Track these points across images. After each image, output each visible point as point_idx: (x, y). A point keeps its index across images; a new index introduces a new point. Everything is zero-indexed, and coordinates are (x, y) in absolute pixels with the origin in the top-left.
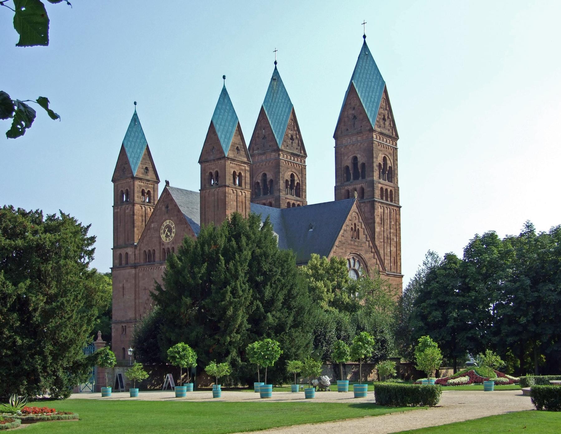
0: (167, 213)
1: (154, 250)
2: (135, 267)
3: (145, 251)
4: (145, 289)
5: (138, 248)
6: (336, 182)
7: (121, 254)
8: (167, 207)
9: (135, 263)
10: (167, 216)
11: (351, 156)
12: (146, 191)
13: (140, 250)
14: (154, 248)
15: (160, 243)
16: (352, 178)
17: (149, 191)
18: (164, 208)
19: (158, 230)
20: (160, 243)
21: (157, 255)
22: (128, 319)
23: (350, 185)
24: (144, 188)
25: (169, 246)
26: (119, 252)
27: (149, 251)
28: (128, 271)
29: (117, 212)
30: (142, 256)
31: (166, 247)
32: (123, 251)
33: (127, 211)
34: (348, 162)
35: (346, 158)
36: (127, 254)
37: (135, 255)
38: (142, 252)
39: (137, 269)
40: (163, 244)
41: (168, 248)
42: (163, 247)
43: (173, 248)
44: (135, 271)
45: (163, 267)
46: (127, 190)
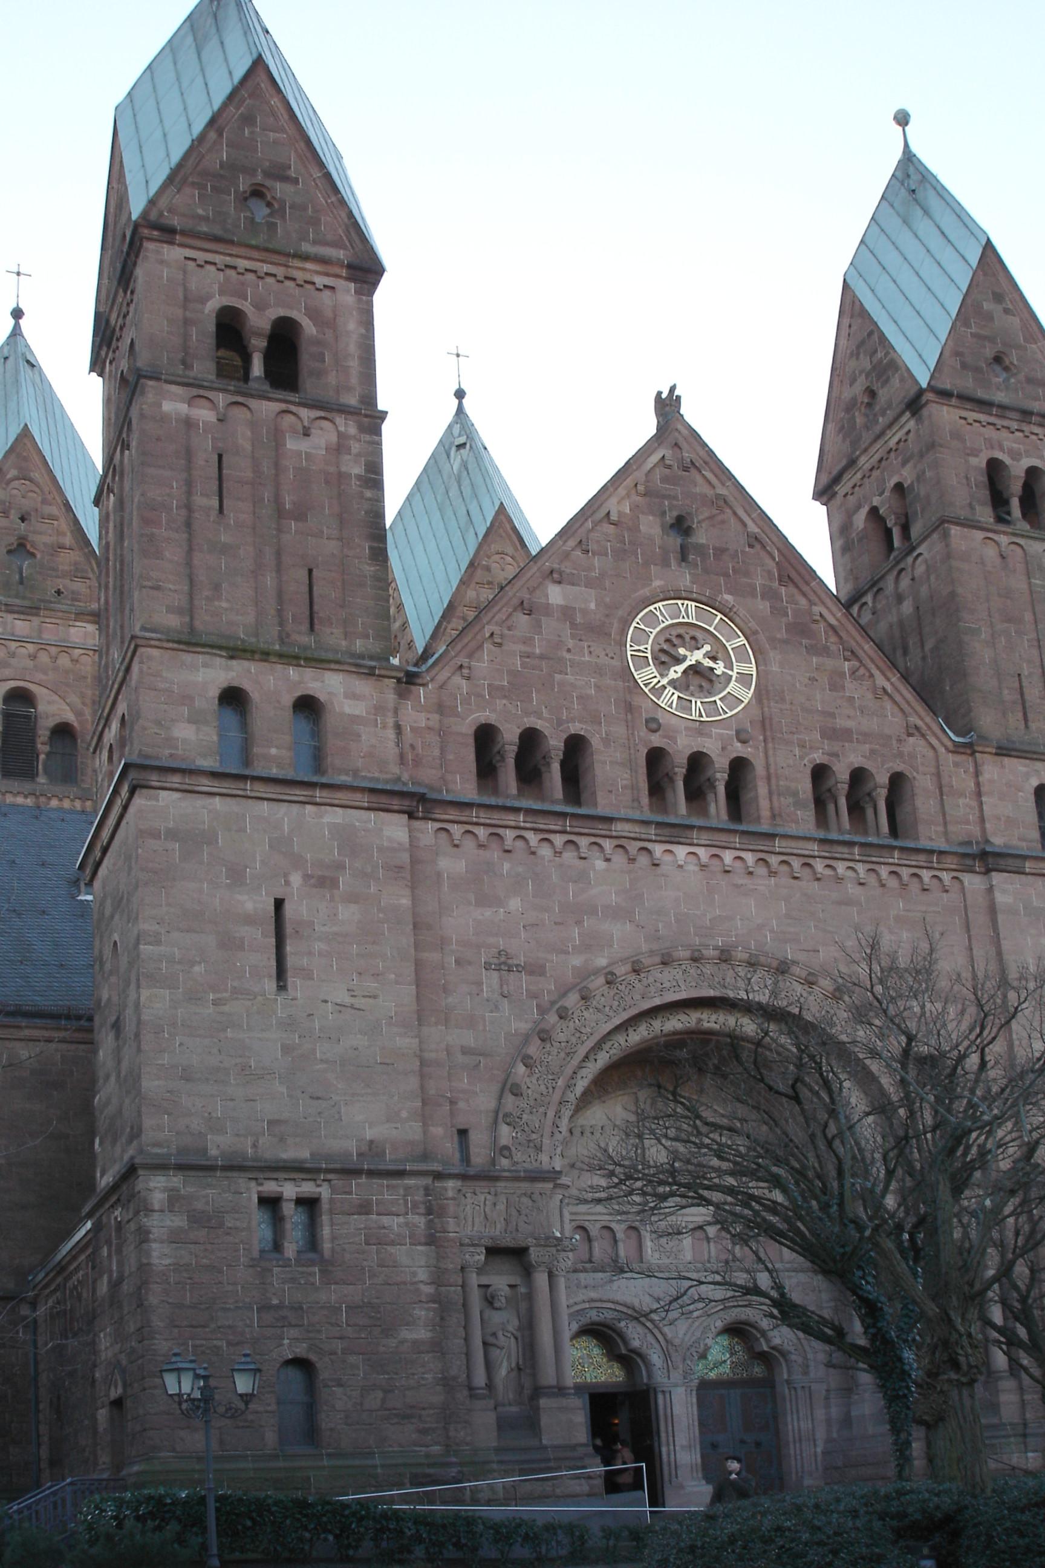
4: (504, 964)
8: (681, 526)
14: (576, 728)
15: (629, 708)
18: (650, 527)
19: (607, 630)
22: (352, 1146)
25: (710, 746)
27: (530, 739)
28: (335, 816)
40: (653, 725)
42: (656, 740)
43: (739, 767)
45: (681, 851)
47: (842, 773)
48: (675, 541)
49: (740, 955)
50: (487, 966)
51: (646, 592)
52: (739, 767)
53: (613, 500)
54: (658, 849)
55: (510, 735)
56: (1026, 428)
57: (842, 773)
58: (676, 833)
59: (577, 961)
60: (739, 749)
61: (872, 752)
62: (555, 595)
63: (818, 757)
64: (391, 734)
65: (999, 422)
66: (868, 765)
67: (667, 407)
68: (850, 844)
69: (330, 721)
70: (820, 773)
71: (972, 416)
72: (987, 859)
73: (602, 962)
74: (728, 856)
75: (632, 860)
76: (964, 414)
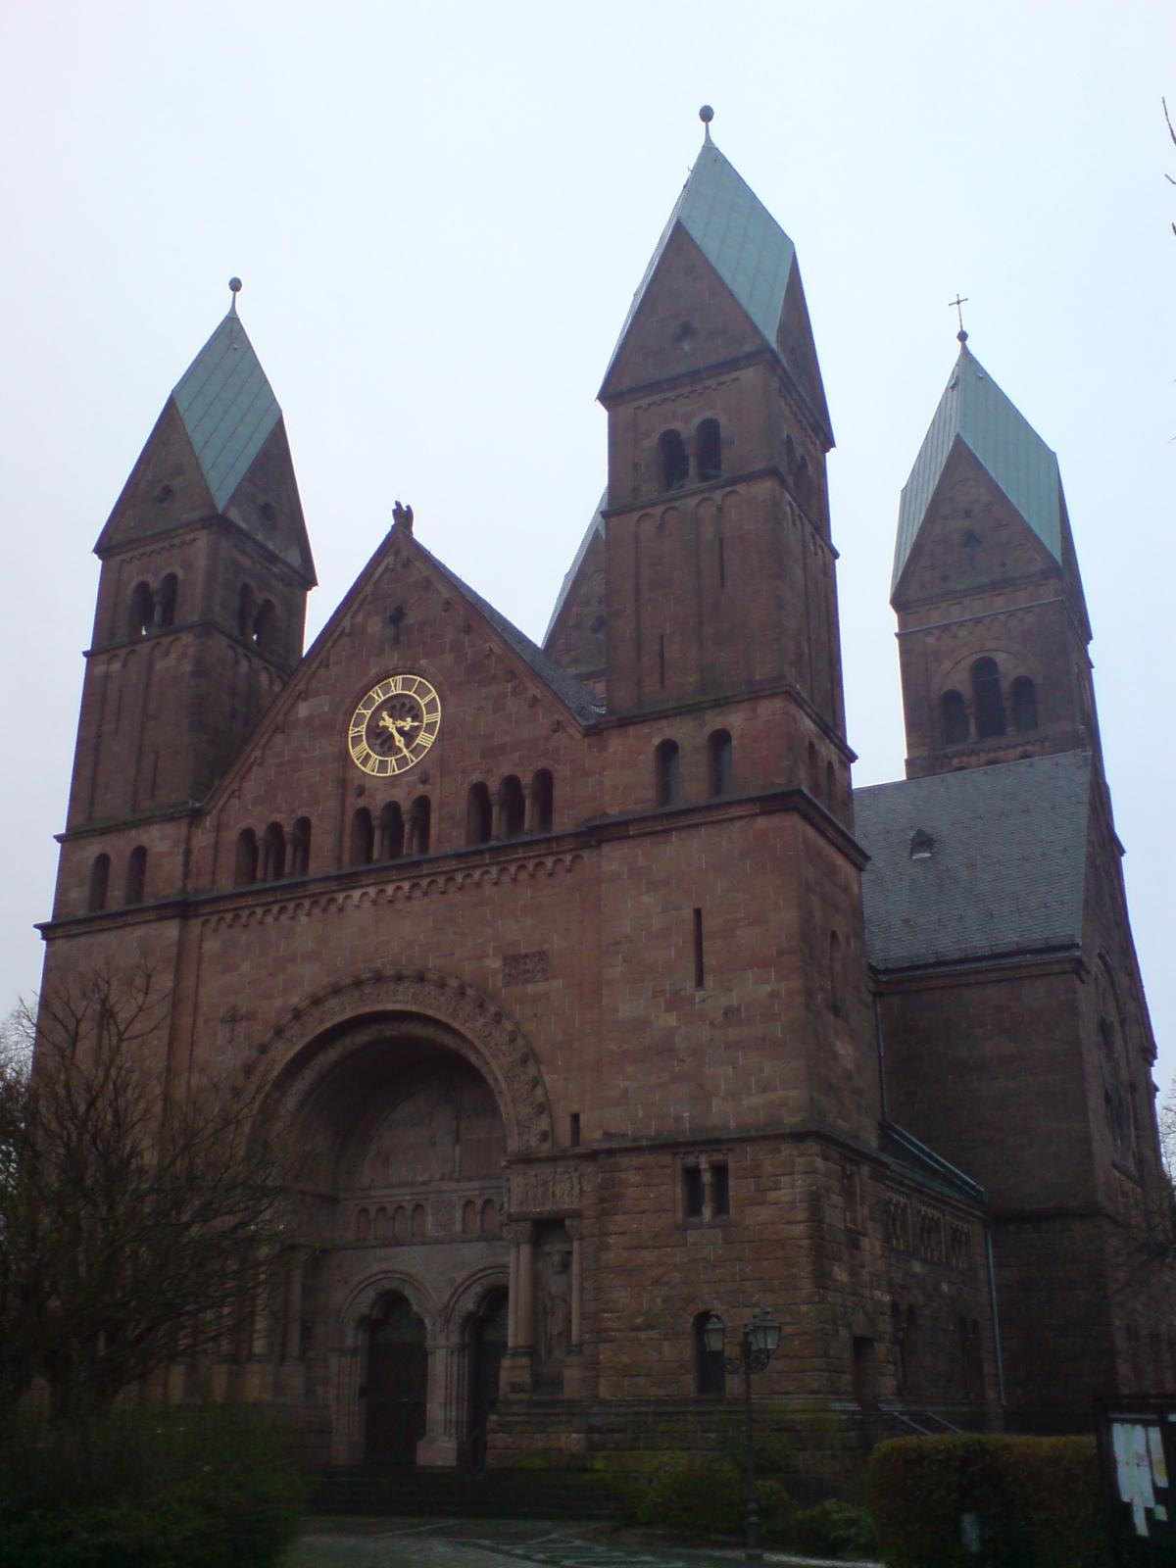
0: (396, 641)
1: (304, 824)
2: (183, 909)
3: (248, 835)
4: (234, 1017)
5: (208, 822)
6: (910, 747)
7: (103, 861)
8: (397, 617)
9: (184, 890)
10: (393, 659)
11: (970, 660)
12: (259, 597)
13: (218, 828)
14: (300, 814)
15: (343, 784)
16: (973, 729)
17: (268, 603)
18: (375, 626)
19: (335, 727)
20: (343, 784)
21: (322, 840)
23: (973, 752)
24: (252, 583)
26: (92, 850)
27: (275, 829)
28: (140, 932)
29: (107, 676)
30: (230, 858)
31: (378, 802)
32: (119, 848)
33: (158, 666)
34: (960, 680)
35: (947, 665)
36: (140, 853)
37: (188, 853)
38: (232, 836)
39: (195, 926)
40: (361, 791)
41: (393, 808)
42: (361, 803)
43: (423, 805)
44: (183, 930)
45: (357, 894)
46: (172, 579)
47: (494, 786)
48: (390, 631)
49: (389, 971)
50: (222, 1021)
51: (364, 682)
52: (423, 805)
53: (348, 618)
54: (341, 897)
55: (260, 831)
56: (699, 387)
57: (494, 786)
58: (348, 881)
59: (278, 1003)
60: (421, 790)
61: (520, 758)
62: (303, 710)
63: (476, 777)
64: (180, 859)
65: (671, 394)
66: (518, 772)
67: (403, 517)
68: (481, 852)
69: (150, 861)
70: (479, 791)
71: (644, 402)
72: (598, 833)
73: (295, 1000)
74: (390, 889)
75: (325, 910)
76: (637, 404)
